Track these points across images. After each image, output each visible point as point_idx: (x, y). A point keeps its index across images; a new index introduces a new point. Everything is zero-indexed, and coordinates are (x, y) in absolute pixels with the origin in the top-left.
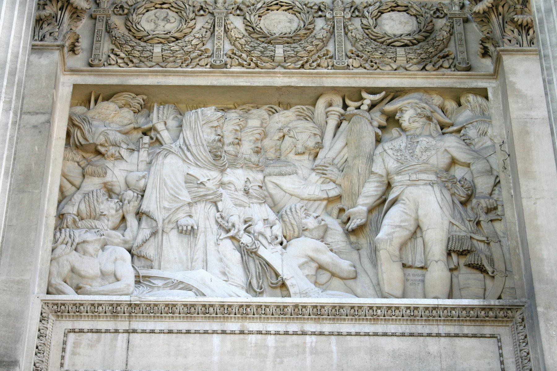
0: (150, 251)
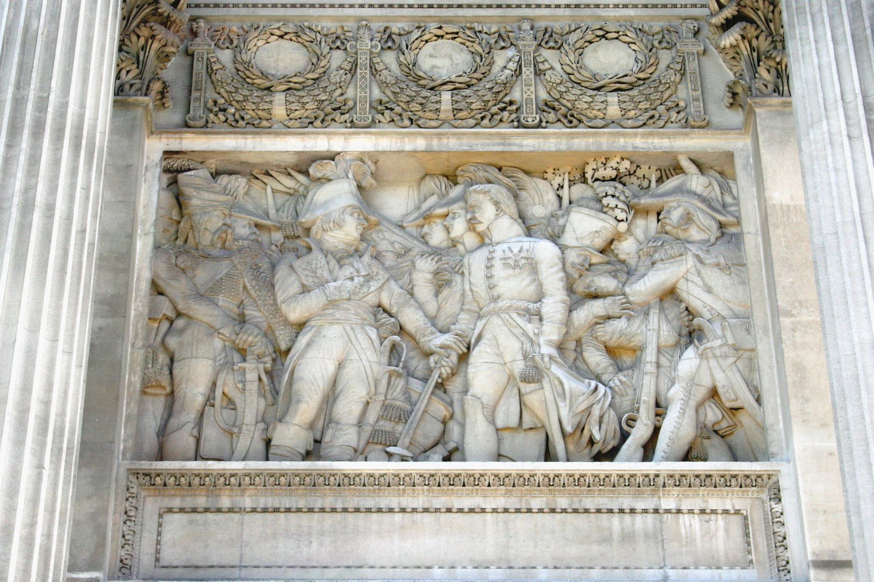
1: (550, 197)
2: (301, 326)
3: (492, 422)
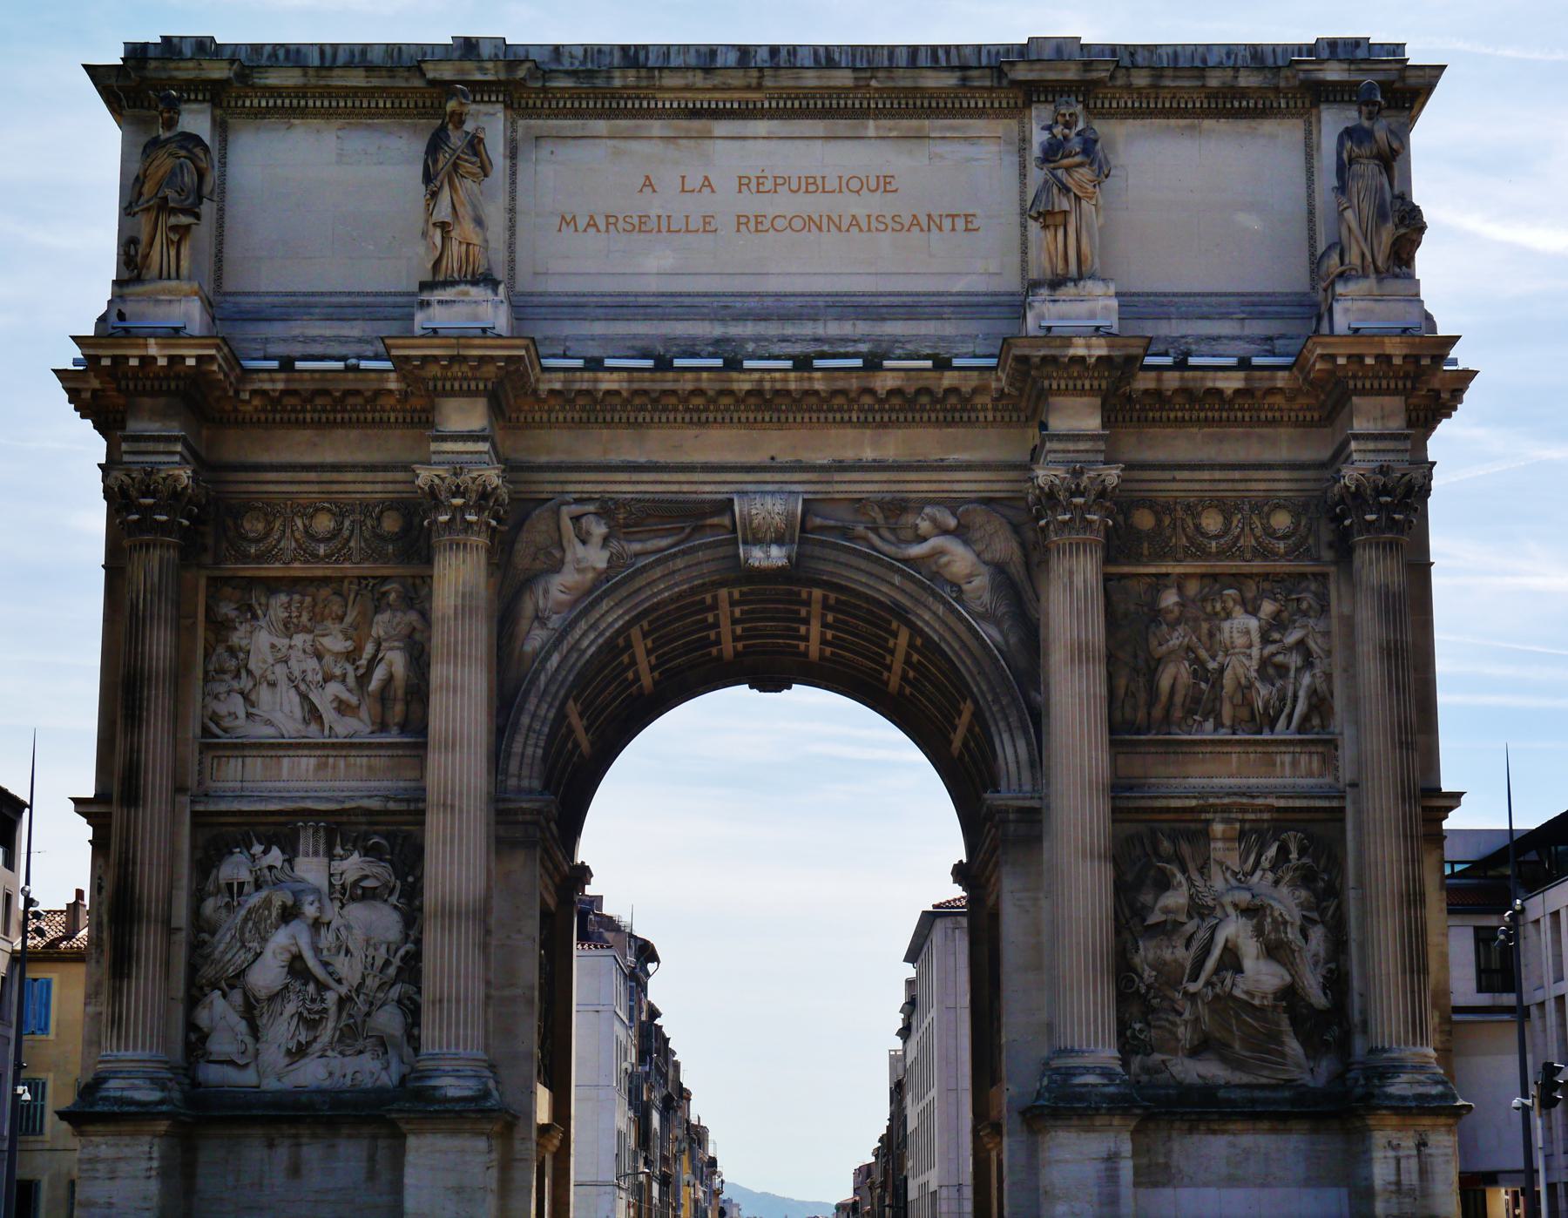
0: (253, 697)
1: (1254, 587)
2: (1160, 659)
3: (1232, 702)
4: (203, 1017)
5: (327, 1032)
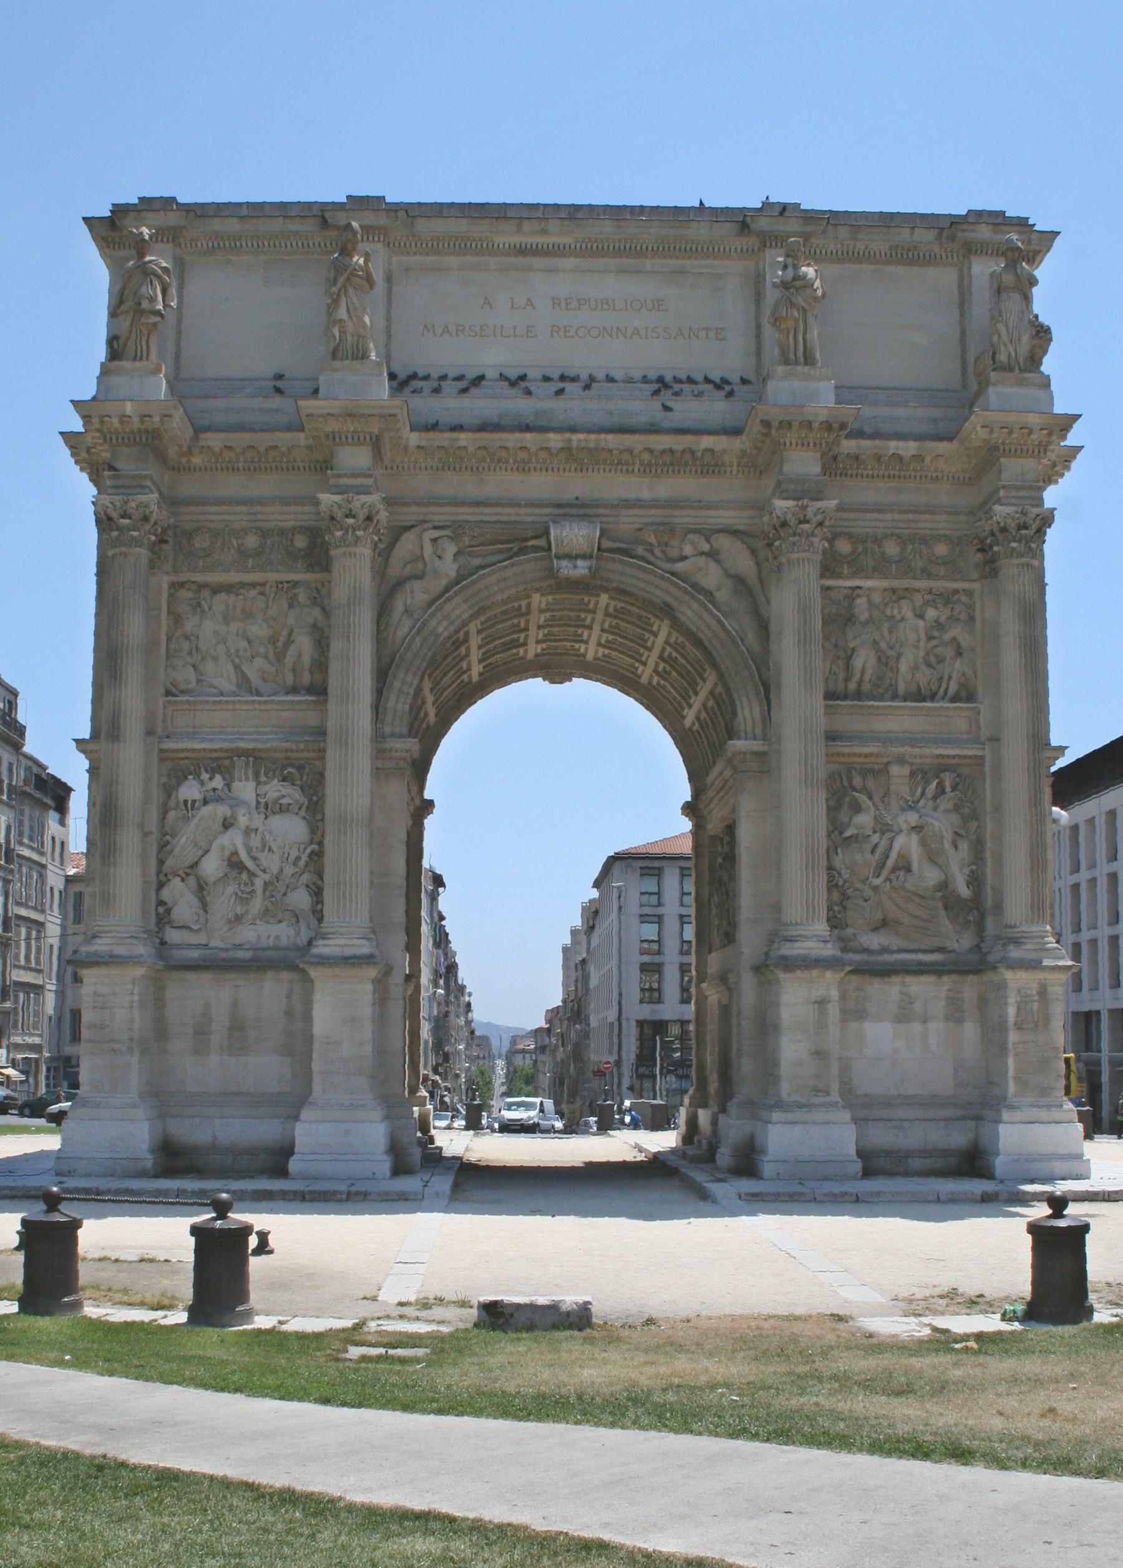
2: (854, 650)
4: (166, 894)
5: (257, 904)
